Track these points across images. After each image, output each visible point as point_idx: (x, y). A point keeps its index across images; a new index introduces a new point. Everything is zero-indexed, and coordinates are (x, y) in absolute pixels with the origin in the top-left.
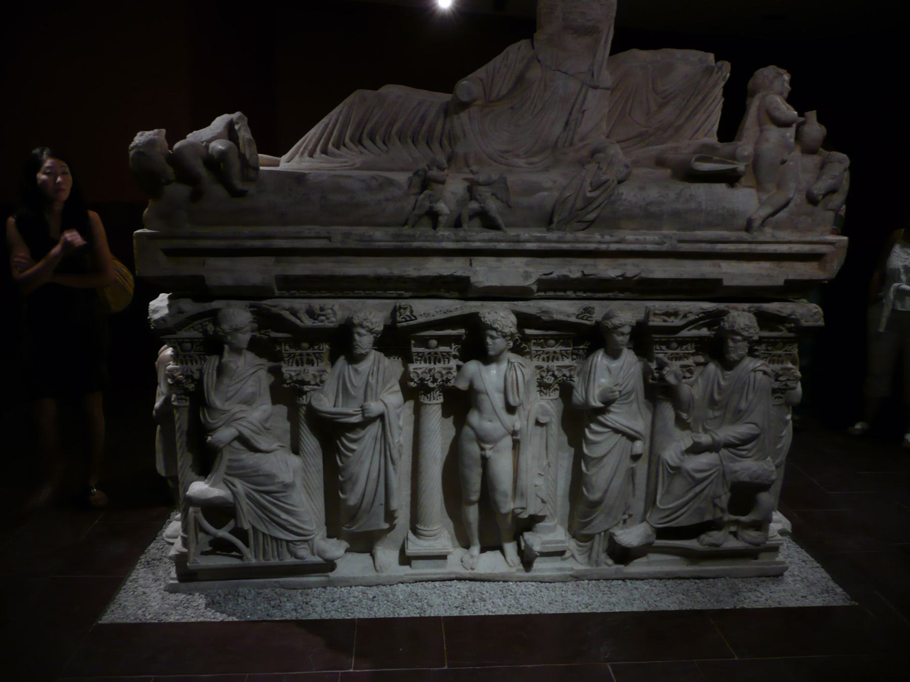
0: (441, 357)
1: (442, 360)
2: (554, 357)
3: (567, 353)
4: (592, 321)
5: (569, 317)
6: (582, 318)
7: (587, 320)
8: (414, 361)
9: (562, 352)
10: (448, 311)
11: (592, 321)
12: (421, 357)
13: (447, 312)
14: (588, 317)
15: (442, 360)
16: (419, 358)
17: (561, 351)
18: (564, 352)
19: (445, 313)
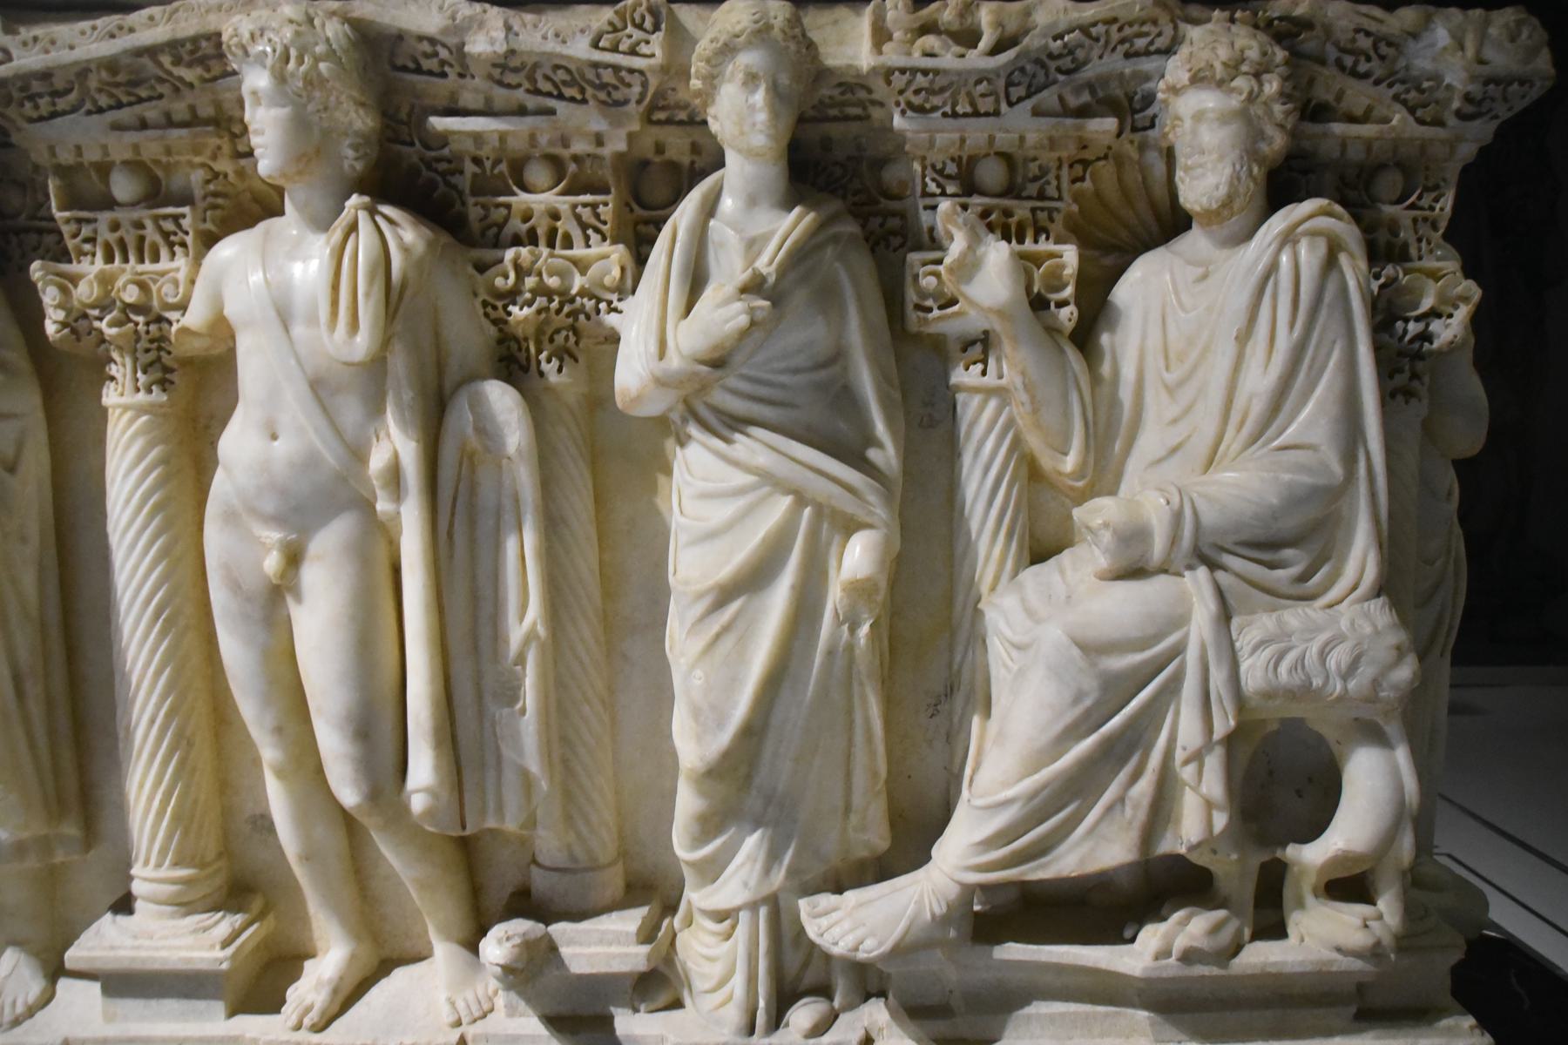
0: (158, 239)
1: (164, 253)
2: (552, 233)
3: (597, 216)
4: (653, 55)
5: (564, 42)
6: (615, 49)
7: (633, 52)
8: (73, 256)
9: (579, 209)
10: (121, 28)
11: (653, 55)
12: (91, 240)
13: (116, 32)
14: (638, 43)
15: (164, 253)
16: (87, 247)
17: (574, 206)
18: (588, 209)
19: (113, 36)
